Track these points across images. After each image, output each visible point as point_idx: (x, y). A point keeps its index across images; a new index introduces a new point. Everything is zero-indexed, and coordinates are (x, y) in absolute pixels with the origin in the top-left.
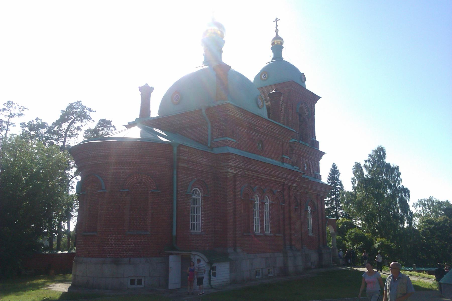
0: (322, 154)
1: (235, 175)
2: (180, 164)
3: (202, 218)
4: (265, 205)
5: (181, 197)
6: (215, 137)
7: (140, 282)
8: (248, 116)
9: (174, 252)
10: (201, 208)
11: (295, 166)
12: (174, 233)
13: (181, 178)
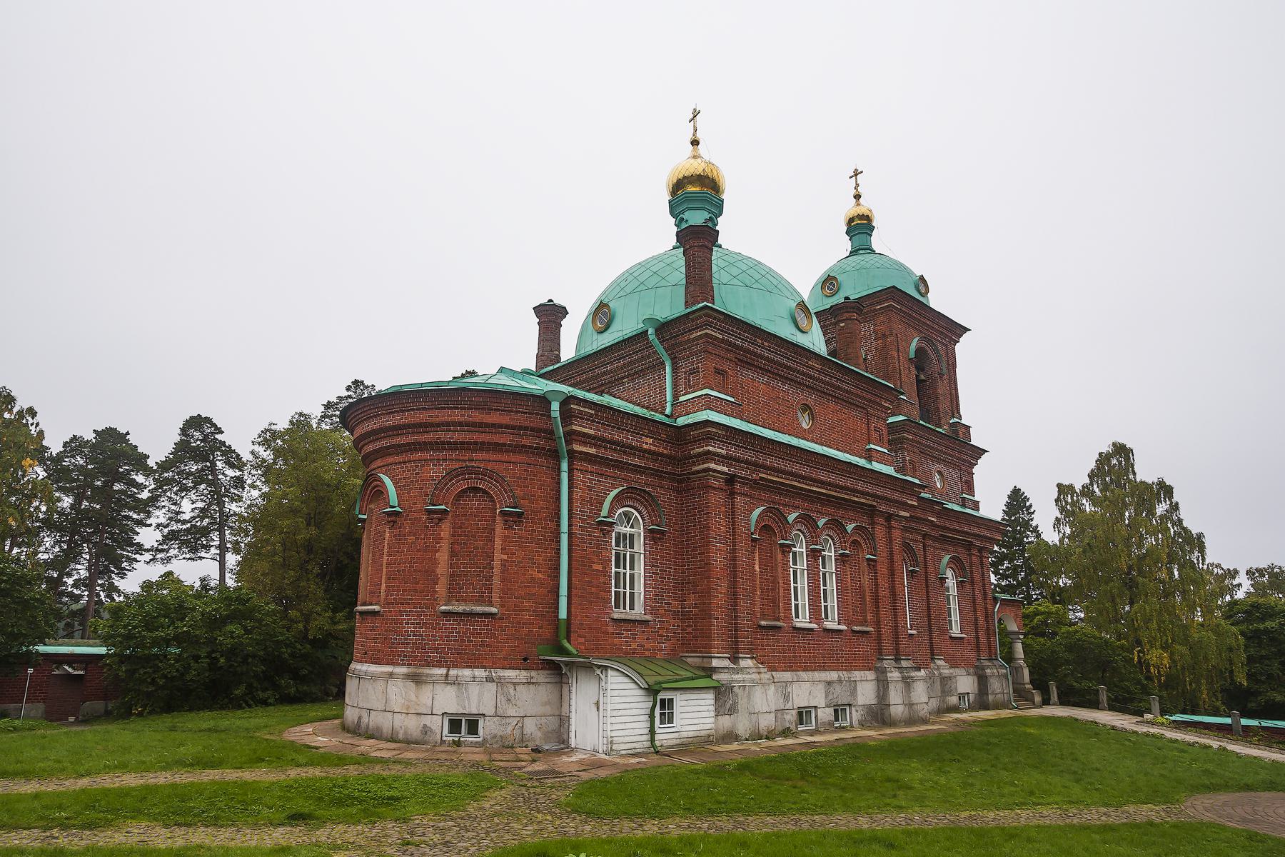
1: (731, 479)
2: (577, 447)
3: (645, 580)
4: (824, 558)
6: (682, 391)
7: (473, 727)
8: (766, 344)
9: (564, 659)
12: (563, 614)
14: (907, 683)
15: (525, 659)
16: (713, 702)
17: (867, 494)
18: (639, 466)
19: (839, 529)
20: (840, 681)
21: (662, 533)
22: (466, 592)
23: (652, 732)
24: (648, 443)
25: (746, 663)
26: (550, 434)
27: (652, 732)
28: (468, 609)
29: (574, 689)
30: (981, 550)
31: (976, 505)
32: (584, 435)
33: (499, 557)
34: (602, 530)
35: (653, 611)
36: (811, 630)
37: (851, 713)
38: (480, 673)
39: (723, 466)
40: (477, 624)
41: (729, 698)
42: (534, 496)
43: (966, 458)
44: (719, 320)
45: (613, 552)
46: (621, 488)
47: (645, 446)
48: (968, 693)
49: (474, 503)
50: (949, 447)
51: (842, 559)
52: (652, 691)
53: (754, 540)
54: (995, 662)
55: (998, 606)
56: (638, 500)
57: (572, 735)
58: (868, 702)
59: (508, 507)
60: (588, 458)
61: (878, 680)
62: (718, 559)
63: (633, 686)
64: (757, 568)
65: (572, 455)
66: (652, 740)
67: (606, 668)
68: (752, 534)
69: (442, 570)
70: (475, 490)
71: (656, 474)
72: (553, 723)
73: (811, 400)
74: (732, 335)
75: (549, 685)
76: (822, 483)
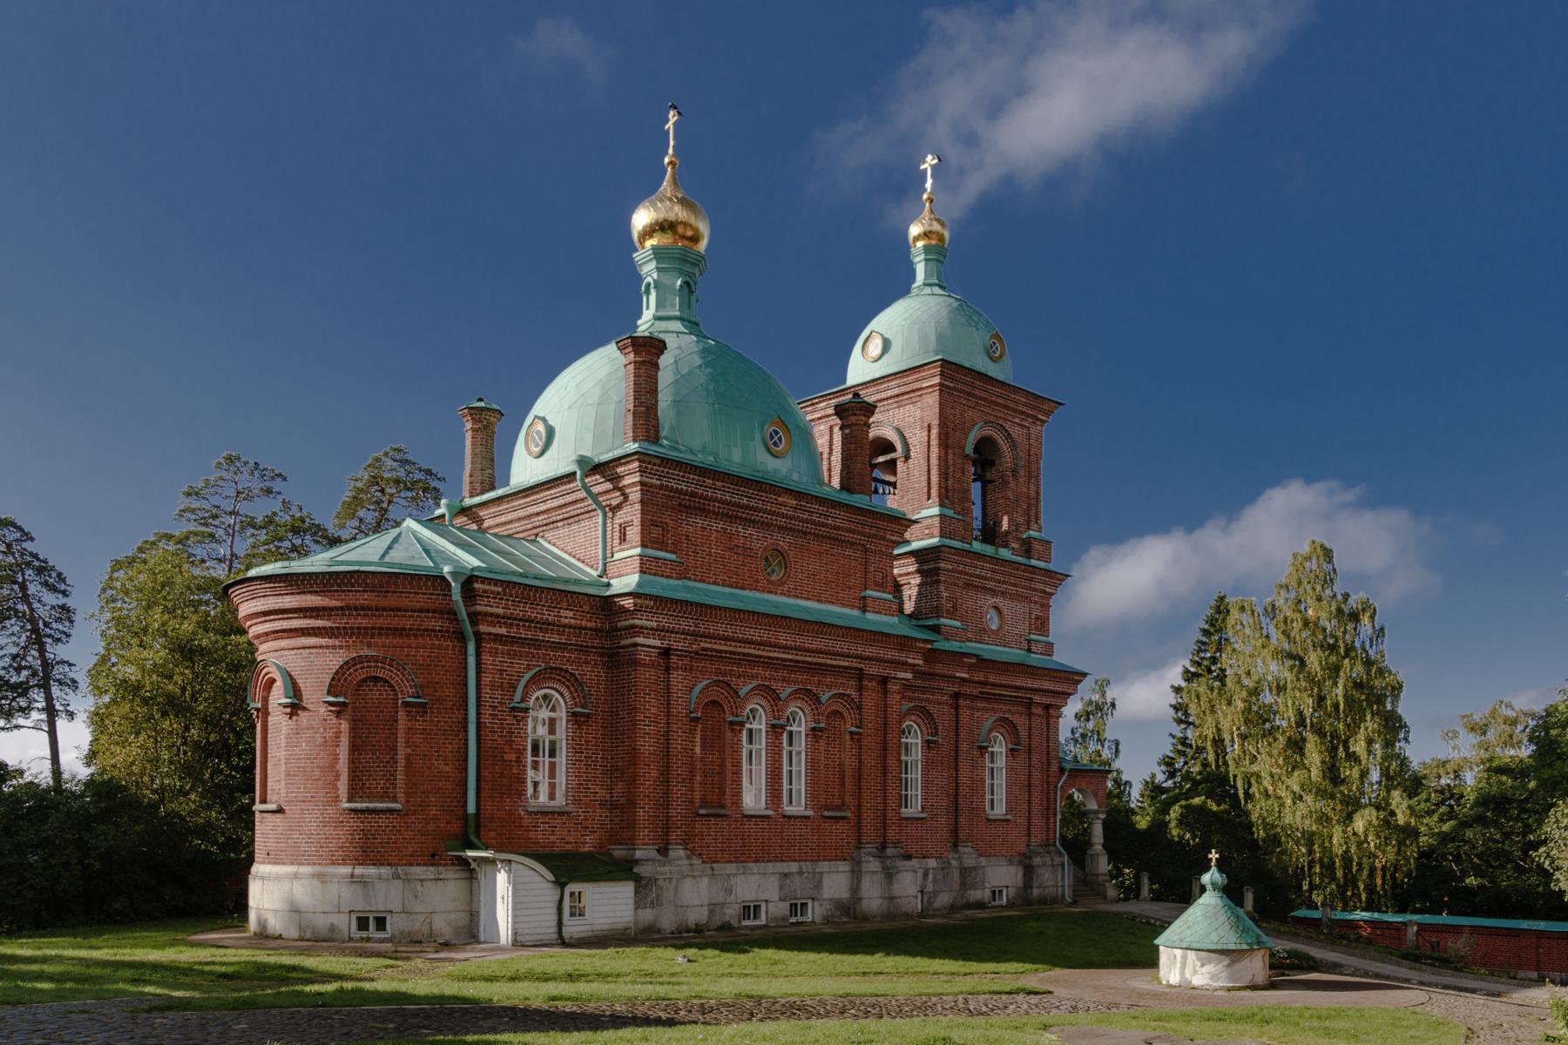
1: (666, 653)
2: (483, 628)
3: (567, 768)
4: (791, 733)
5: (490, 714)
7: (381, 923)
10: (564, 742)
11: (943, 617)
12: (471, 809)
13: (491, 665)
14: (889, 875)
15: (433, 856)
16: (632, 895)
17: (849, 656)
18: (559, 643)
19: (811, 700)
20: (800, 873)
21: (588, 716)
22: (369, 788)
23: (560, 924)
24: (567, 616)
25: (677, 852)
26: (452, 614)
27: (560, 924)
28: (371, 805)
29: (482, 884)
30: (1047, 707)
31: (1049, 649)
32: (491, 615)
34: (515, 717)
35: (576, 801)
36: (768, 817)
37: (813, 908)
38: (385, 871)
40: (383, 821)
41: (651, 890)
43: (1038, 586)
45: (529, 740)
46: (538, 669)
47: (566, 621)
49: (376, 693)
51: (814, 733)
52: (561, 885)
53: (696, 720)
54: (1052, 848)
56: (559, 680)
57: (482, 929)
58: (836, 896)
59: (409, 696)
60: (498, 638)
61: (853, 872)
62: (647, 745)
63: (541, 879)
64: (698, 750)
65: (479, 636)
66: (560, 932)
67: (510, 861)
68: (691, 712)
70: (376, 679)
71: (584, 649)
72: (461, 919)
73: (784, 542)
74: (674, 479)
75: (458, 881)
76: (785, 648)
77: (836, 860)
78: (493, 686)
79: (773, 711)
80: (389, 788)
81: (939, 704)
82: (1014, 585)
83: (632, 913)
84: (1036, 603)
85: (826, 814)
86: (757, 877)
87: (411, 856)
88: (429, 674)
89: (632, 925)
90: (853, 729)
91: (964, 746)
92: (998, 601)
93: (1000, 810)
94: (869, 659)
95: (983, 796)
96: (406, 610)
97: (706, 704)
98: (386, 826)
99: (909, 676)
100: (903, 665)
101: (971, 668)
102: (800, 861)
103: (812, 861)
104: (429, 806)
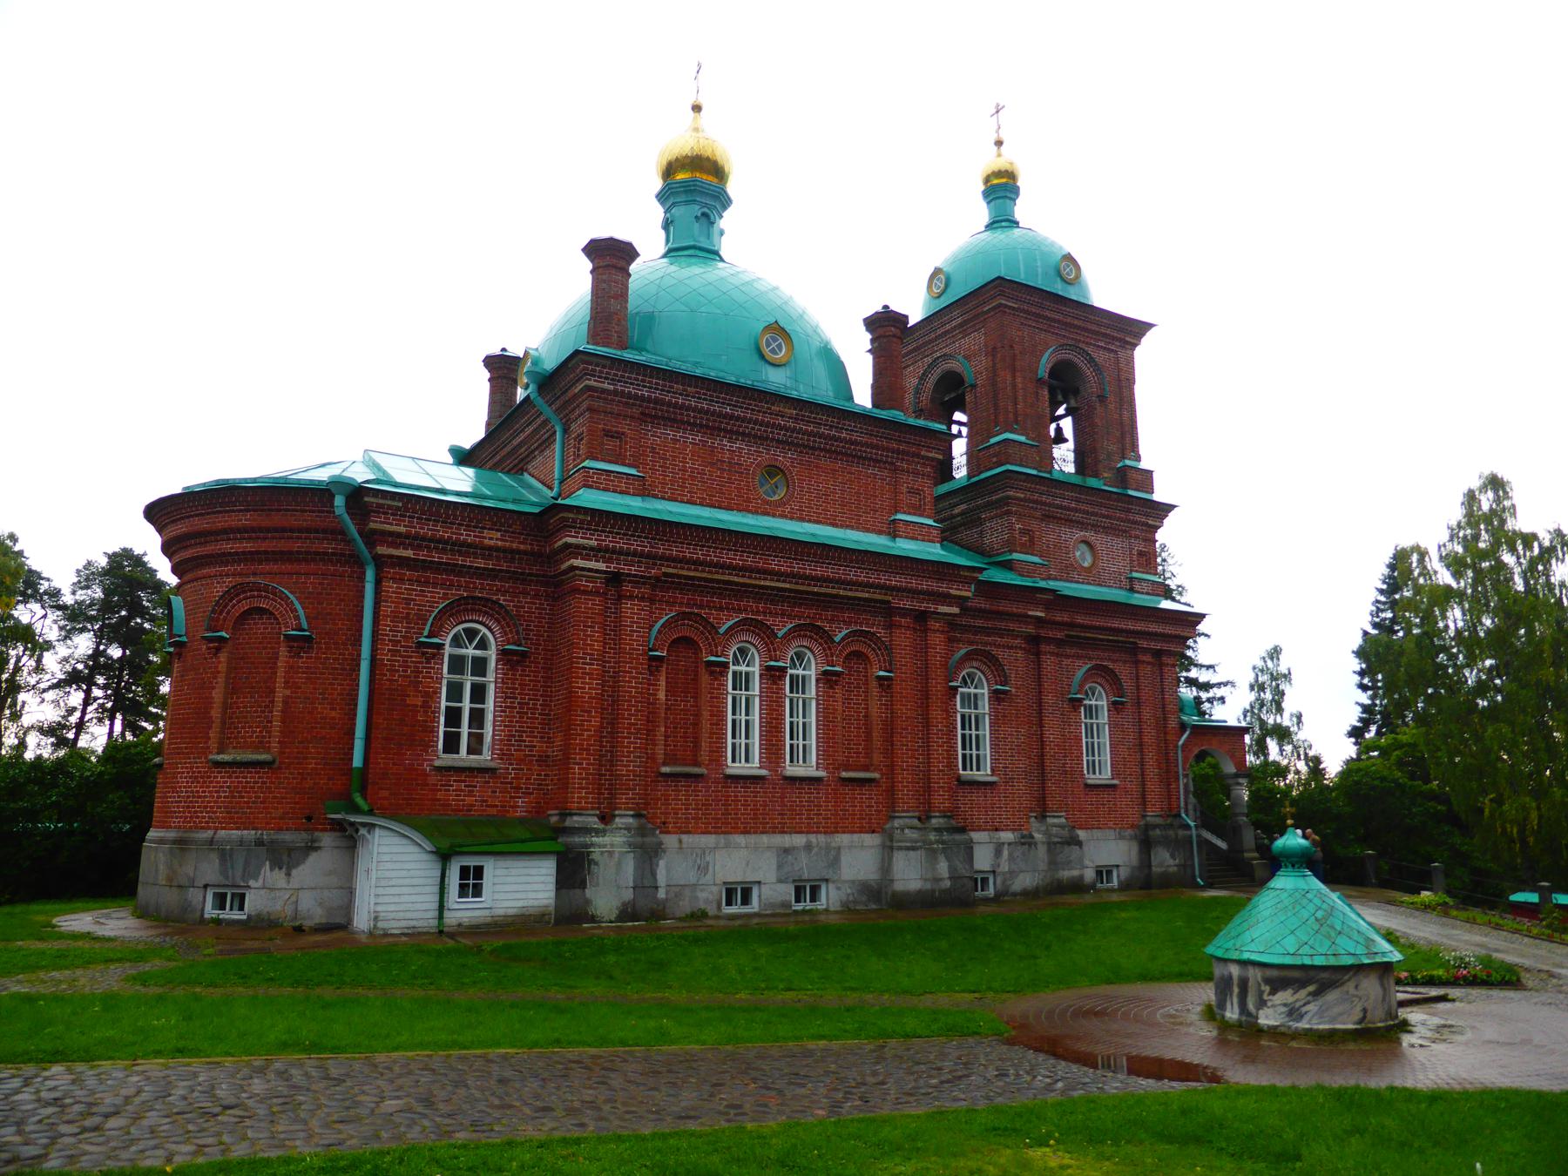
0: (1164, 510)
1: (614, 579)
3: (495, 716)
5: (389, 650)
12: (357, 761)
13: (393, 592)
16: (554, 871)
17: (871, 586)
18: (484, 569)
19: (822, 638)
20: (808, 847)
21: (523, 654)
23: (441, 908)
24: (493, 538)
27: (441, 908)
30: (1158, 654)
32: (391, 534)
33: (281, 693)
34: (424, 653)
39: (597, 561)
40: (251, 777)
42: (330, 614)
44: (604, 367)
45: (445, 682)
47: (486, 541)
48: (1118, 866)
50: (1102, 505)
51: (826, 679)
52: (444, 857)
55: (1185, 736)
58: (862, 876)
60: (403, 562)
61: (883, 846)
62: (587, 688)
63: (415, 849)
64: (662, 695)
65: (380, 562)
66: (441, 917)
67: (374, 826)
68: (651, 650)
69: (216, 713)
77: (861, 832)
78: (395, 617)
79: (769, 650)
80: (264, 737)
81: (1011, 648)
82: (1107, 517)
83: (552, 894)
84: (1137, 537)
85: (844, 774)
86: (744, 853)
87: (281, 818)
88: (318, 603)
89: (552, 909)
90: (882, 673)
91: (1049, 699)
92: (1089, 535)
93: (1105, 775)
94: (898, 589)
95: (1080, 757)
96: (291, 531)
97: (674, 641)
98: (255, 782)
99: (956, 610)
100: (946, 598)
101: (1048, 606)
102: (808, 832)
103: (825, 833)
104: (306, 758)
